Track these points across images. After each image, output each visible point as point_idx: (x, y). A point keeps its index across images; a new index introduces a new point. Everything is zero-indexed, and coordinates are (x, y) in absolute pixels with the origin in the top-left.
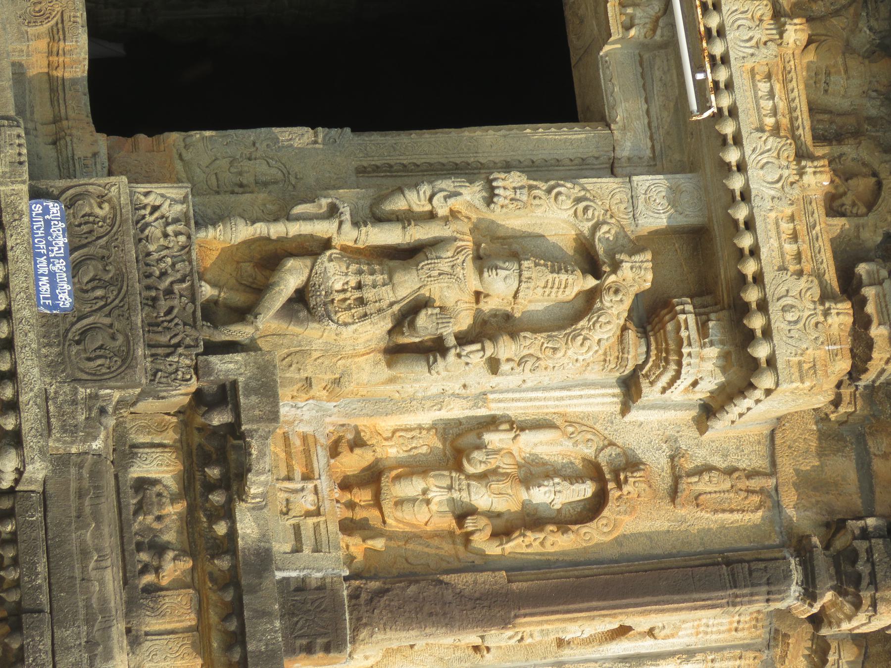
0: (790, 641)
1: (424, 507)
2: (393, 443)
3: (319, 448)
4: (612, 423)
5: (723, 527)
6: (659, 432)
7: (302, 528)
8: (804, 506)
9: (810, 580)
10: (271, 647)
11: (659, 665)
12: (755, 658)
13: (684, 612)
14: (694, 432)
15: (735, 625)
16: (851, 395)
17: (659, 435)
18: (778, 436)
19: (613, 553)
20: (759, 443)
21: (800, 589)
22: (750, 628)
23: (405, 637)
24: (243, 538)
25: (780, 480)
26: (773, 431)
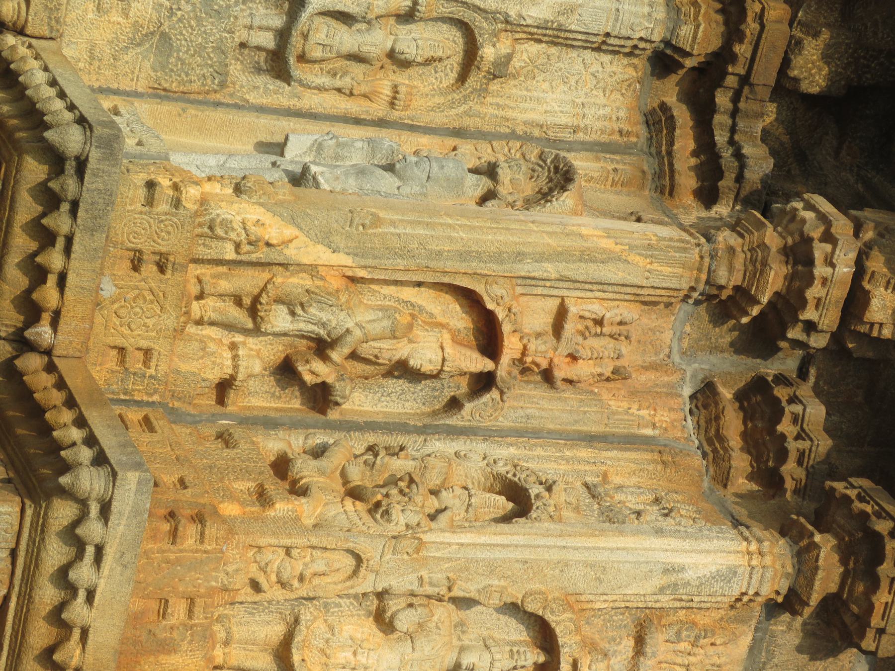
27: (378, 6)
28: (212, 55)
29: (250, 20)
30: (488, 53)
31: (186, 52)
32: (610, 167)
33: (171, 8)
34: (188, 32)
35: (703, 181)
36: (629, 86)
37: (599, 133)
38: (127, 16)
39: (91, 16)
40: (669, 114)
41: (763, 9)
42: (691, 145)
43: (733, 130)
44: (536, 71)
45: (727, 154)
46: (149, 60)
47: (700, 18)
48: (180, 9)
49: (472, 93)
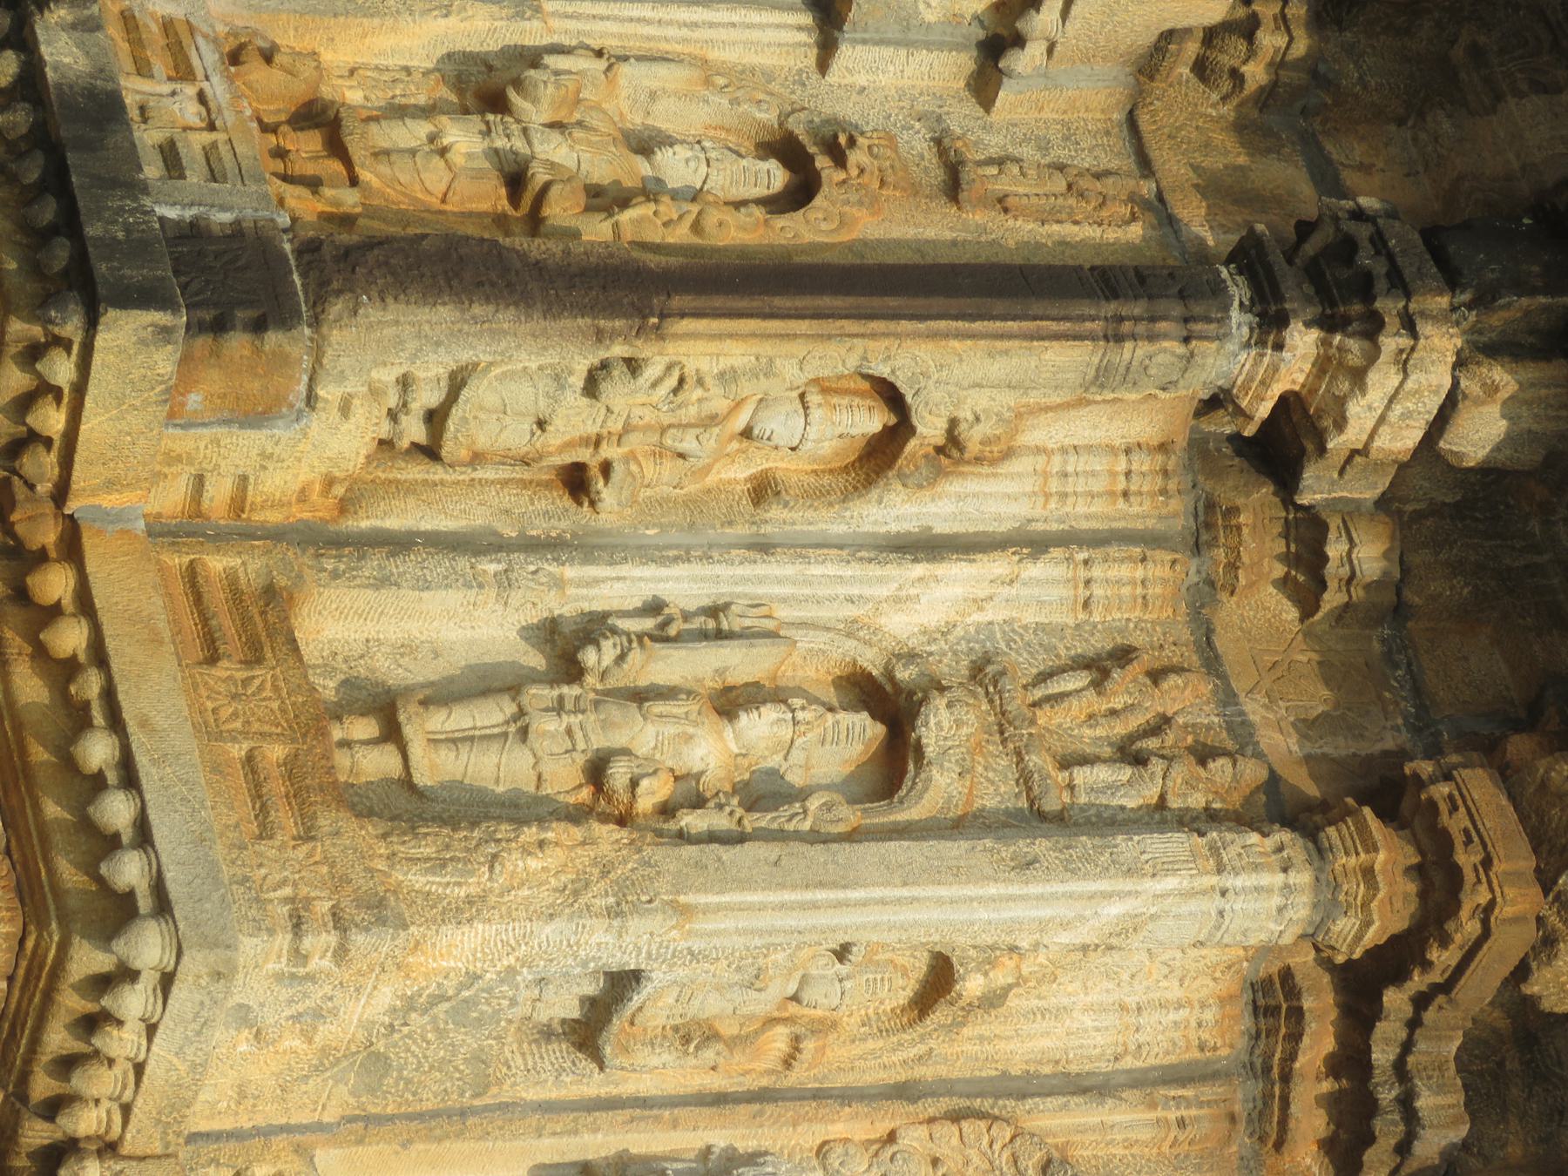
0: (1242, 519)
1: (437, 162)
2: (355, 83)
3: (200, 41)
4: (804, 85)
5: (1063, 243)
6: (901, 104)
7: (179, 145)
8: (1223, 226)
9: (1267, 290)
10: (136, 235)
11: (974, 560)
12: (1174, 562)
13: (1004, 528)
14: (971, 108)
15: (1121, 484)
16: (1275, 18)
17: (903, 108)
18: (1144, 119)
19: (851, 259)
20: (1108, 133)
21: (1249, 317)
22: (1152, 495)
23: (428, 322)
24: (55, 69)
25: (1164, 183)
26: (1131, 112)
27: (776, 965)
28: (462, 1067)
29: (537, 992)
30: (972, 985)
31: (416, 1070)
32: (1173, 1115)
33: (391, 1025)
34: (420, 1047)
35: (1338, 1125)
36: (1229, 967)
37: (1161, 1055)
38: (310, 1041)
39: (243, 1047)
40: (1295, 1003)
41: (1492, 904)
42: (1329, 1045)
43: (1407, 1047)
44: (1059, 972)
45: (1387, 1095)
46: (346, 1084)
47: (1374, 905)
48: (406, 1024)
49: (936, 1030)
